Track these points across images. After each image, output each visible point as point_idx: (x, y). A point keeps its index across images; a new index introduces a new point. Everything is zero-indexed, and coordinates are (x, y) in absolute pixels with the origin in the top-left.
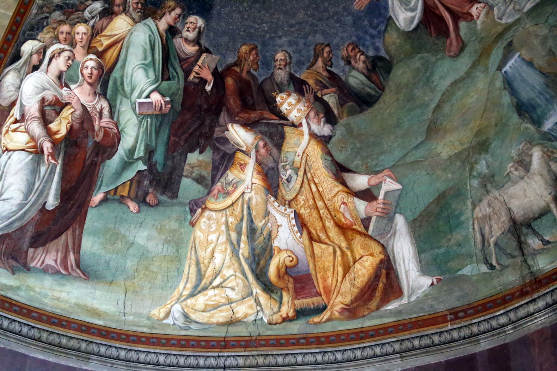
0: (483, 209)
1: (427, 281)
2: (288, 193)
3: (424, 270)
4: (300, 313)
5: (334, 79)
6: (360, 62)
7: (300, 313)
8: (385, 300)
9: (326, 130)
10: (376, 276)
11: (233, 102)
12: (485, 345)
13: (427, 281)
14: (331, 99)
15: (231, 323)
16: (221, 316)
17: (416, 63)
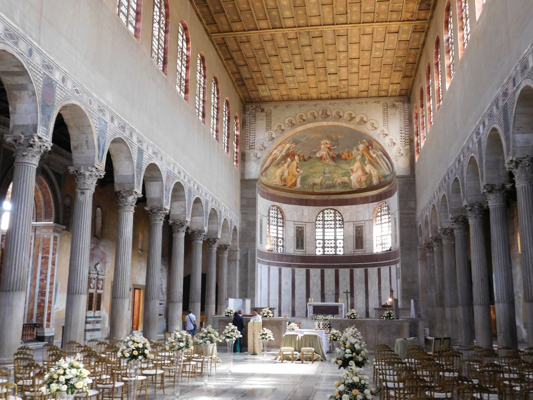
0: (311, 180)
1: (300, 186)
2: (289, 168)
3: (300, 184)
4: (284, 185)
5: (303, 156)
6: (308, 156)
7: (284, 185)
8: (294, 187)
9: (298, 162)
10: (294, 183)
11: (291, 155)
12: (305, 198)
13: (300, 186)
14: (301, 159)
15: (276, 185)
16: (275, 184)
17: (315, 160)
